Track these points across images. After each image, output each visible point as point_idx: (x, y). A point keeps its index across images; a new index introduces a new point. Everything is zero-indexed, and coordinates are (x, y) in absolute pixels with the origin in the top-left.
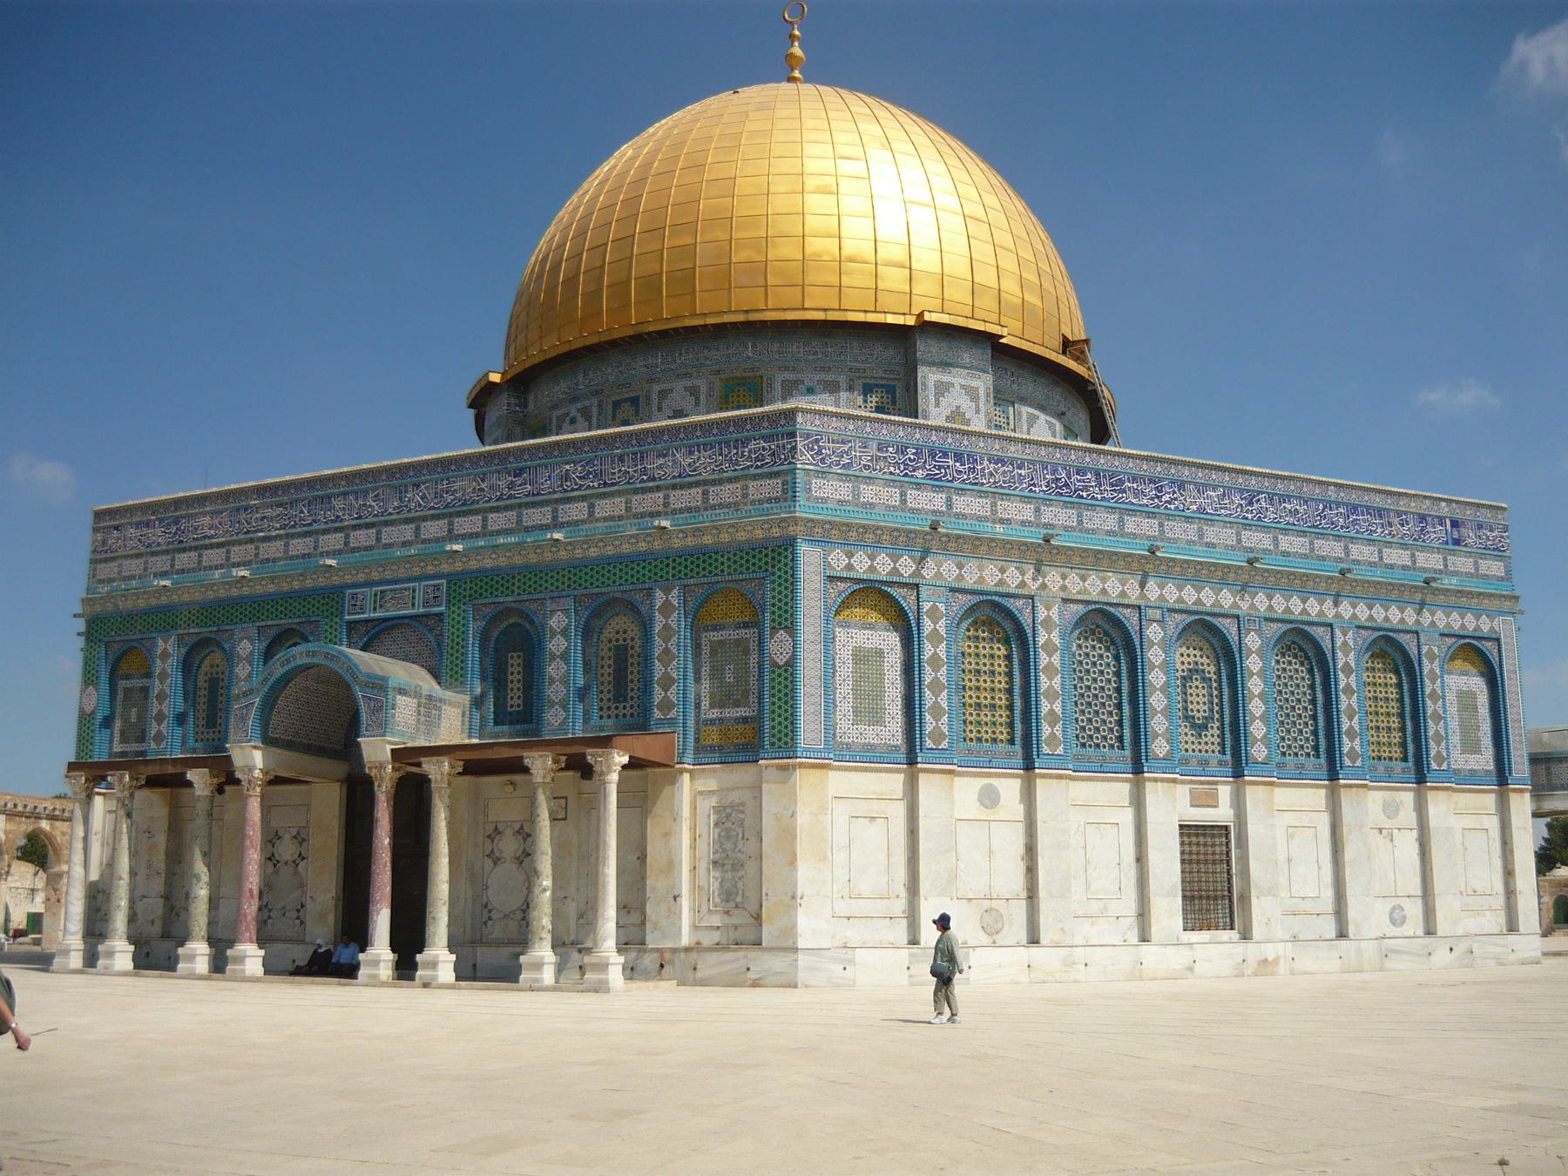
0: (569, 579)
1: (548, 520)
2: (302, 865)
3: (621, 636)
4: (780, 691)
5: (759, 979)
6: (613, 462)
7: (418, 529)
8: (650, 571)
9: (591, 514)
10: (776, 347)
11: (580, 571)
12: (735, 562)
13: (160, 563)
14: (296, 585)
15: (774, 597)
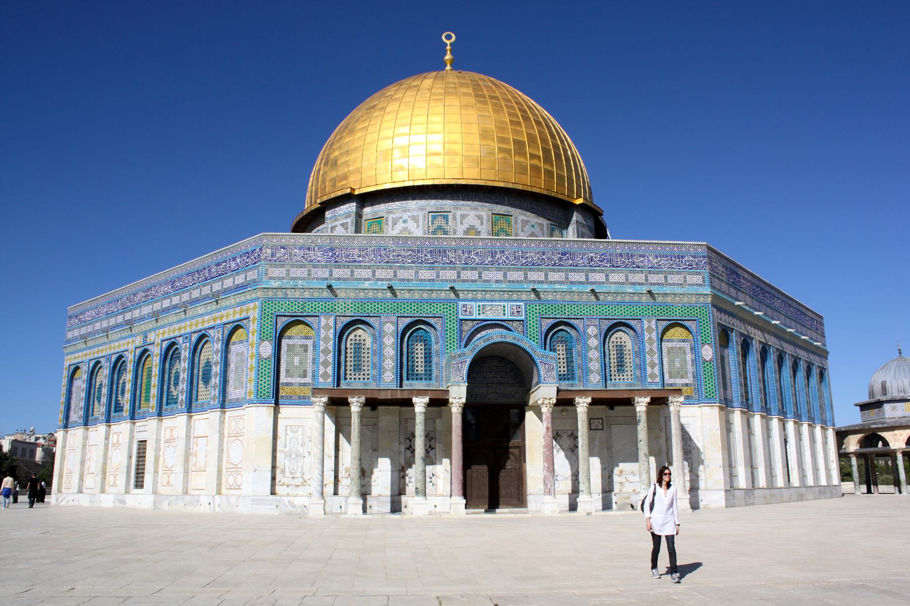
0: (597, 310)
1: (583, 279)
2: (432, 453)
3: (619, 340)
4: (708, 372)
5: (707, 505)
6: (616, 256)
7: (505, 275)
8: (640, 311)
9: (607, 278)
10: (518, 202)
11: (602, 307)
12: (682, 311)
13: (323, 273)
14: (425, 295)
15: (702, 329)
